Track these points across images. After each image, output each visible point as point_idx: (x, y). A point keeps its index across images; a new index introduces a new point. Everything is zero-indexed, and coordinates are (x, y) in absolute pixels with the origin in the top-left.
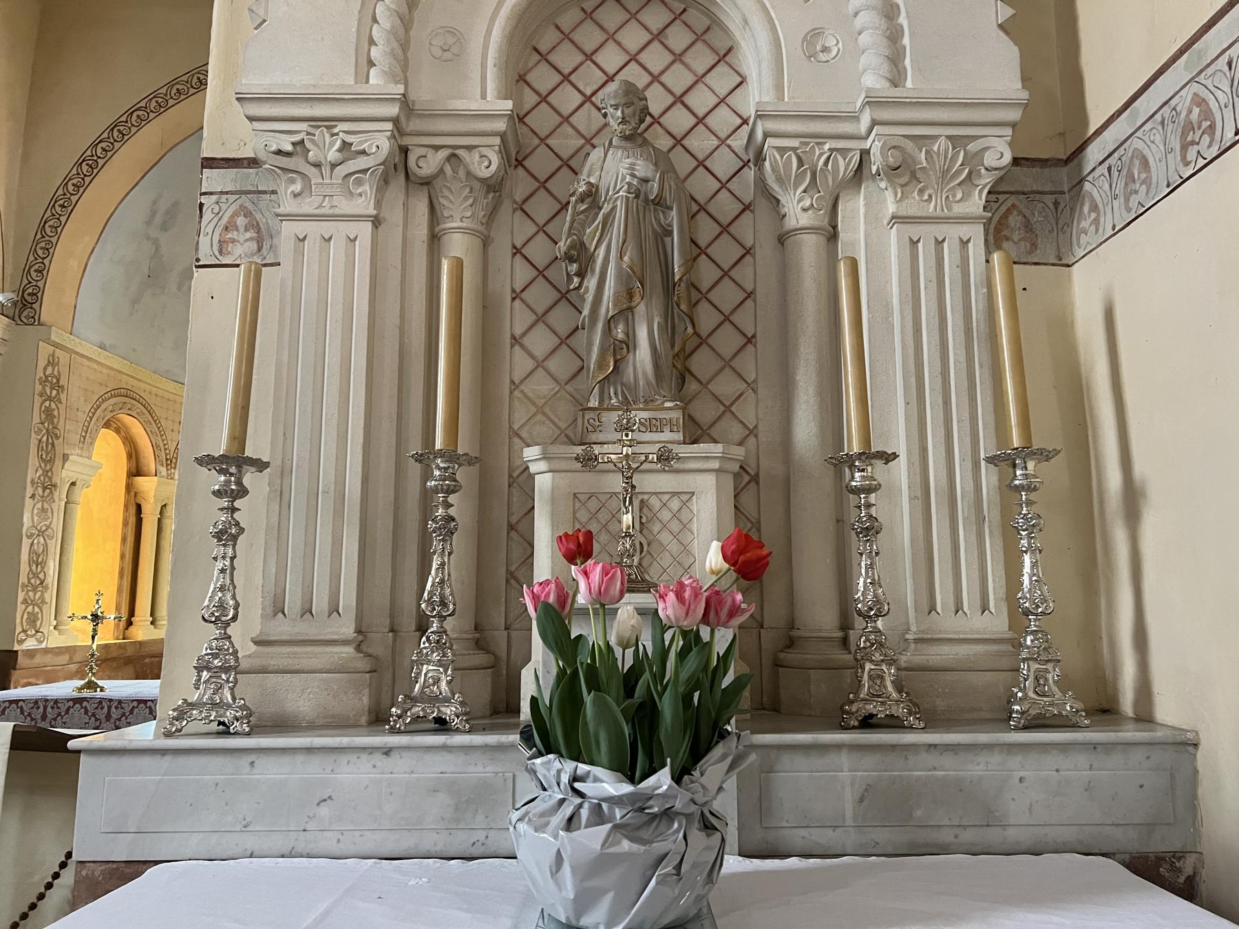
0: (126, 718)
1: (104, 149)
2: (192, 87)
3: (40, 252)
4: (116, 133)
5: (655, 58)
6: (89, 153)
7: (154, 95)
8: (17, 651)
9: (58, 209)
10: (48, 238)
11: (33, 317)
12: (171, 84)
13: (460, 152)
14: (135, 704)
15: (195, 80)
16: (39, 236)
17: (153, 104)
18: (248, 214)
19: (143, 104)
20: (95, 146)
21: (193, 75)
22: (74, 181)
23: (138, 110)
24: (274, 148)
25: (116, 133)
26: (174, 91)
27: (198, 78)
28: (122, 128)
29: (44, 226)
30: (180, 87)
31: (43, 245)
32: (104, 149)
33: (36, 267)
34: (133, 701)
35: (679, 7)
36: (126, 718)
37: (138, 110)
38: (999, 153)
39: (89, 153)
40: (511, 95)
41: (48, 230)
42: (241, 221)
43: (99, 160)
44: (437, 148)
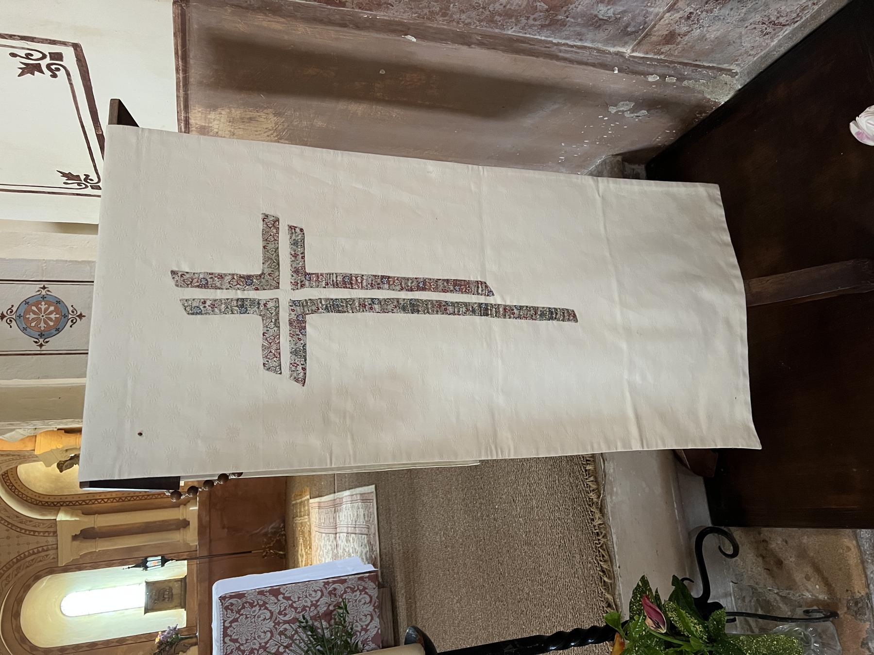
0: (242, 645)
14: (227, 639)
34: (224, 643)
36: (242, 645)
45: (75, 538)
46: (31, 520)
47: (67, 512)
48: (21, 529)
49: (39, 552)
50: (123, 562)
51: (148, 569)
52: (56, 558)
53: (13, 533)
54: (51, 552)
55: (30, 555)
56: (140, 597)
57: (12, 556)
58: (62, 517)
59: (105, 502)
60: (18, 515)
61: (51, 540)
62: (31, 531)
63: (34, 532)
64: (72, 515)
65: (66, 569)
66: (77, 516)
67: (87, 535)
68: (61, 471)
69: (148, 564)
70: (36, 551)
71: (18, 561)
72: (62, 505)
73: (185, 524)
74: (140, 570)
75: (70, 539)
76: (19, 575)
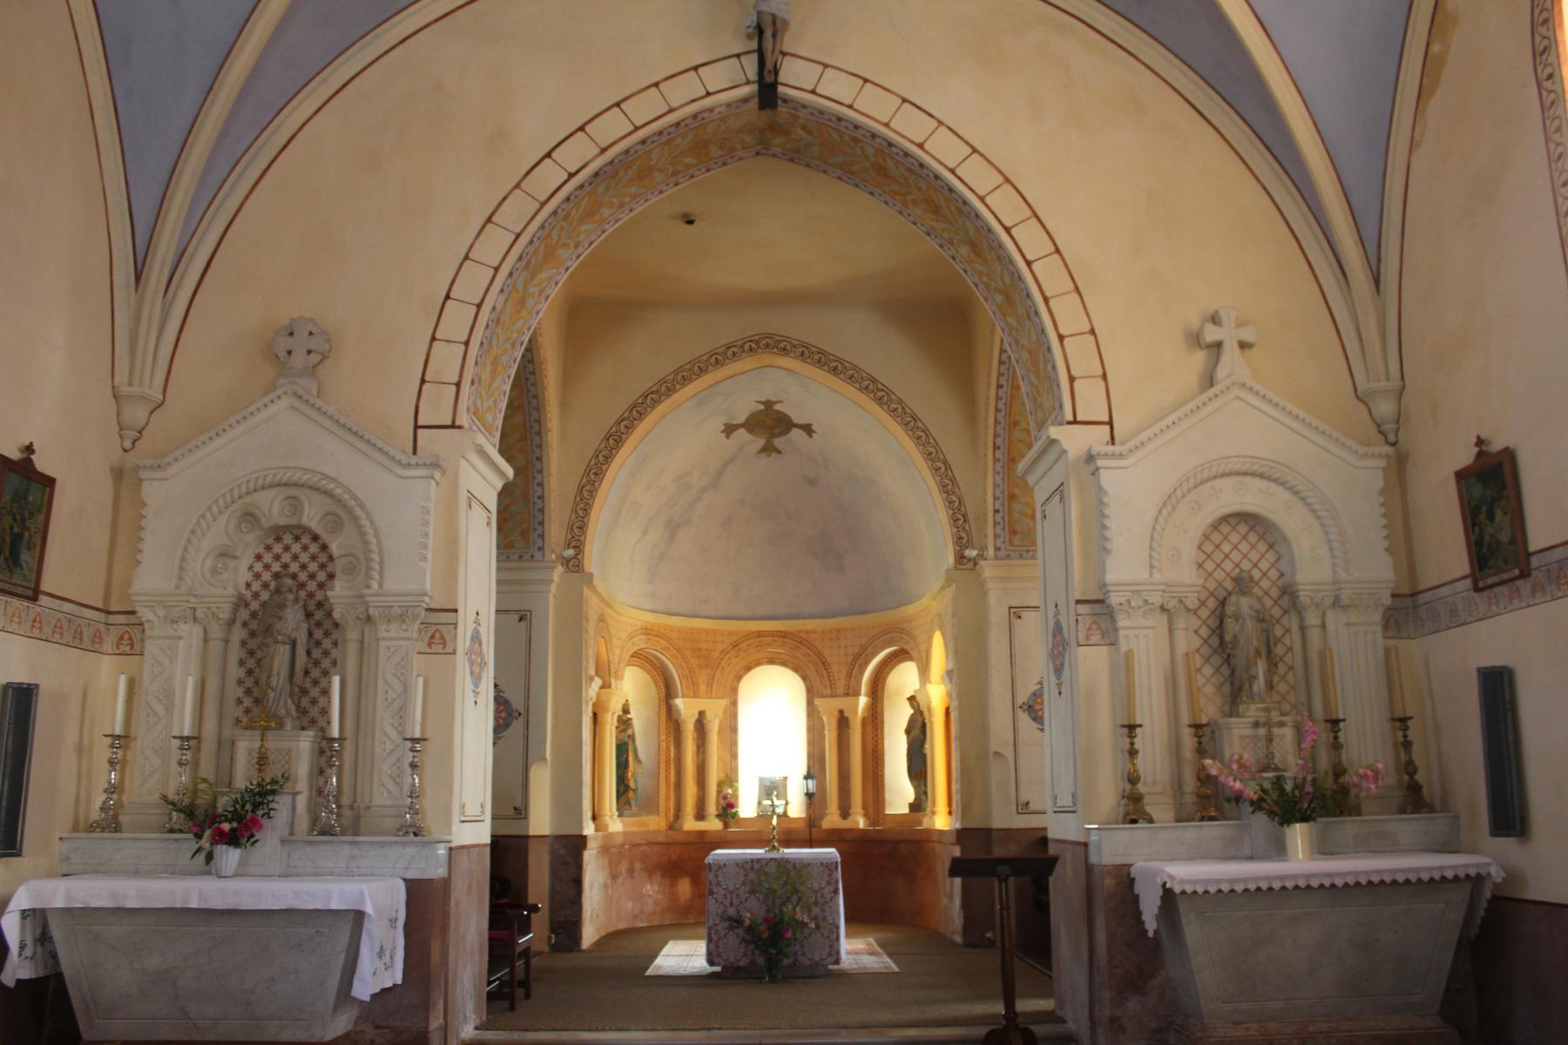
1: (626, 427)
2: (694, 374)
3: (580, 512)
4: (634, 413)
5: (1244, 547)
6: (614, 430)
7: (663, 381)
8: (585, 837)
9: (592, 477)
10: (585, 501)
11: (578, 566)
12: (676, 372)
13: (1183, 599)
15: (696, 368)
16: (578, 498)
17: (664, 388)
18: (1096, 623)
19: (655, 388)
20: (618, 423)
21: (694, 364)
22: (604, 453)
23: (651, 393)
24: (1118, 602)
25: (634, 413)
26: (680, 377)
27: (699, 367)
28: (639, 409)
29: (581, 491)
30: (685, 374)
31: (582, 506)
32: (626, 427)
33: (578, 524)
35: (1251, 523)
37: (651, 393)
38: (1388, 601)
39: (614, 430)
40: (1043, 452)
41: (585, 493)
42: (1094, 626)
43: (623, 436)
44: (1174, 597)
45: (841, 712)
46: (862, 673)
47: (866, 704)
48: (854, 666)
49: (830, 680)
50: (810, 756)
51: (805, 781)
52: (823, 696)
53: (850, 659)
54: (828, 692)
55: (828, 673)
56: (775, 774)
57: (829, 659)
58: (863, 701)
59: (873, 738)
60: (867, 663)
61: (841, 691)
62: (851, 674)
63: (850, 677)
64: (864, 709)
65: (810, 703)
66: (863, 713)
67: (843, 722)
68: (908, 699)
69: (810, 781)
70: (832, 678)
71: (823, 663)
72: (873, 699)
73: (845, 812)
74: (804, 771)
75: (841, 708)
76: (810, 665)
